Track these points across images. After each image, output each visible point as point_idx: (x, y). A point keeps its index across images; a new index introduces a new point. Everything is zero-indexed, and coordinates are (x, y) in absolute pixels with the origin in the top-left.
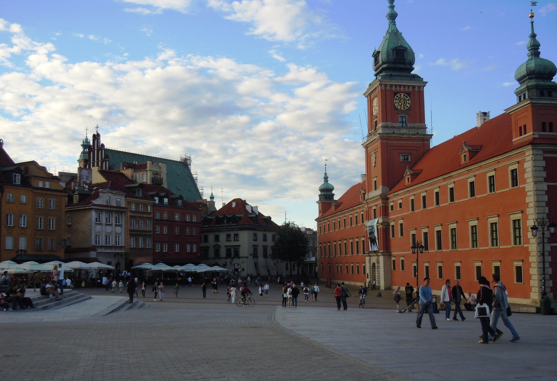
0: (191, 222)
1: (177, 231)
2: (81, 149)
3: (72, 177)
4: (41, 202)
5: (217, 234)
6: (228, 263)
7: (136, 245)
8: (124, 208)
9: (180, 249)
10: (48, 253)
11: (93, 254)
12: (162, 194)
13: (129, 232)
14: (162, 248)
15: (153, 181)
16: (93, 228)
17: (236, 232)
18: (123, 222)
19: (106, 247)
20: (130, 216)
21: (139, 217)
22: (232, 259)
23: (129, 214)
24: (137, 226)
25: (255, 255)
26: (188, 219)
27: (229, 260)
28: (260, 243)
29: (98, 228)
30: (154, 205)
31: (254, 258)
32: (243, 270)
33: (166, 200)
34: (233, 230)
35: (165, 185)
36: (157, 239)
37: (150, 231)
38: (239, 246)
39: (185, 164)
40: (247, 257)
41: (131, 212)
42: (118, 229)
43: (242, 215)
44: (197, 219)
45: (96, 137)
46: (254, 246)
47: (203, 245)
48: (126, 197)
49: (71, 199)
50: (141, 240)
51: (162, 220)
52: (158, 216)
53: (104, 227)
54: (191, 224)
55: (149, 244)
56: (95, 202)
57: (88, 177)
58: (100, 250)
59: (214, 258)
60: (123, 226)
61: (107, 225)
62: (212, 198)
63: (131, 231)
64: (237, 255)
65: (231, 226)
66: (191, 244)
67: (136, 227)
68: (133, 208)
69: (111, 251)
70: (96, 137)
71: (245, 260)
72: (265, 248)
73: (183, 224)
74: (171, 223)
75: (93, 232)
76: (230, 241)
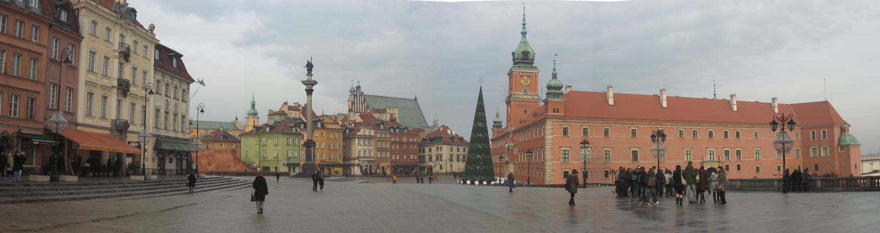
1: (405, 147)
3: (346, 118)
11: (357, 162)
25: (451, 160)
28: (455, 152)
29: (360, 148)
33: (397, 130)
35: (398, 121)
36: (393, 152)
45: (358, 88)
47: (422, 154)
49: (345, 132)
50: (384, 153)
52: (393, 139)
54: (413, 143)
68: (379, 135)
70: (358, 88)
72: (458, 156)
73: (408, 143)
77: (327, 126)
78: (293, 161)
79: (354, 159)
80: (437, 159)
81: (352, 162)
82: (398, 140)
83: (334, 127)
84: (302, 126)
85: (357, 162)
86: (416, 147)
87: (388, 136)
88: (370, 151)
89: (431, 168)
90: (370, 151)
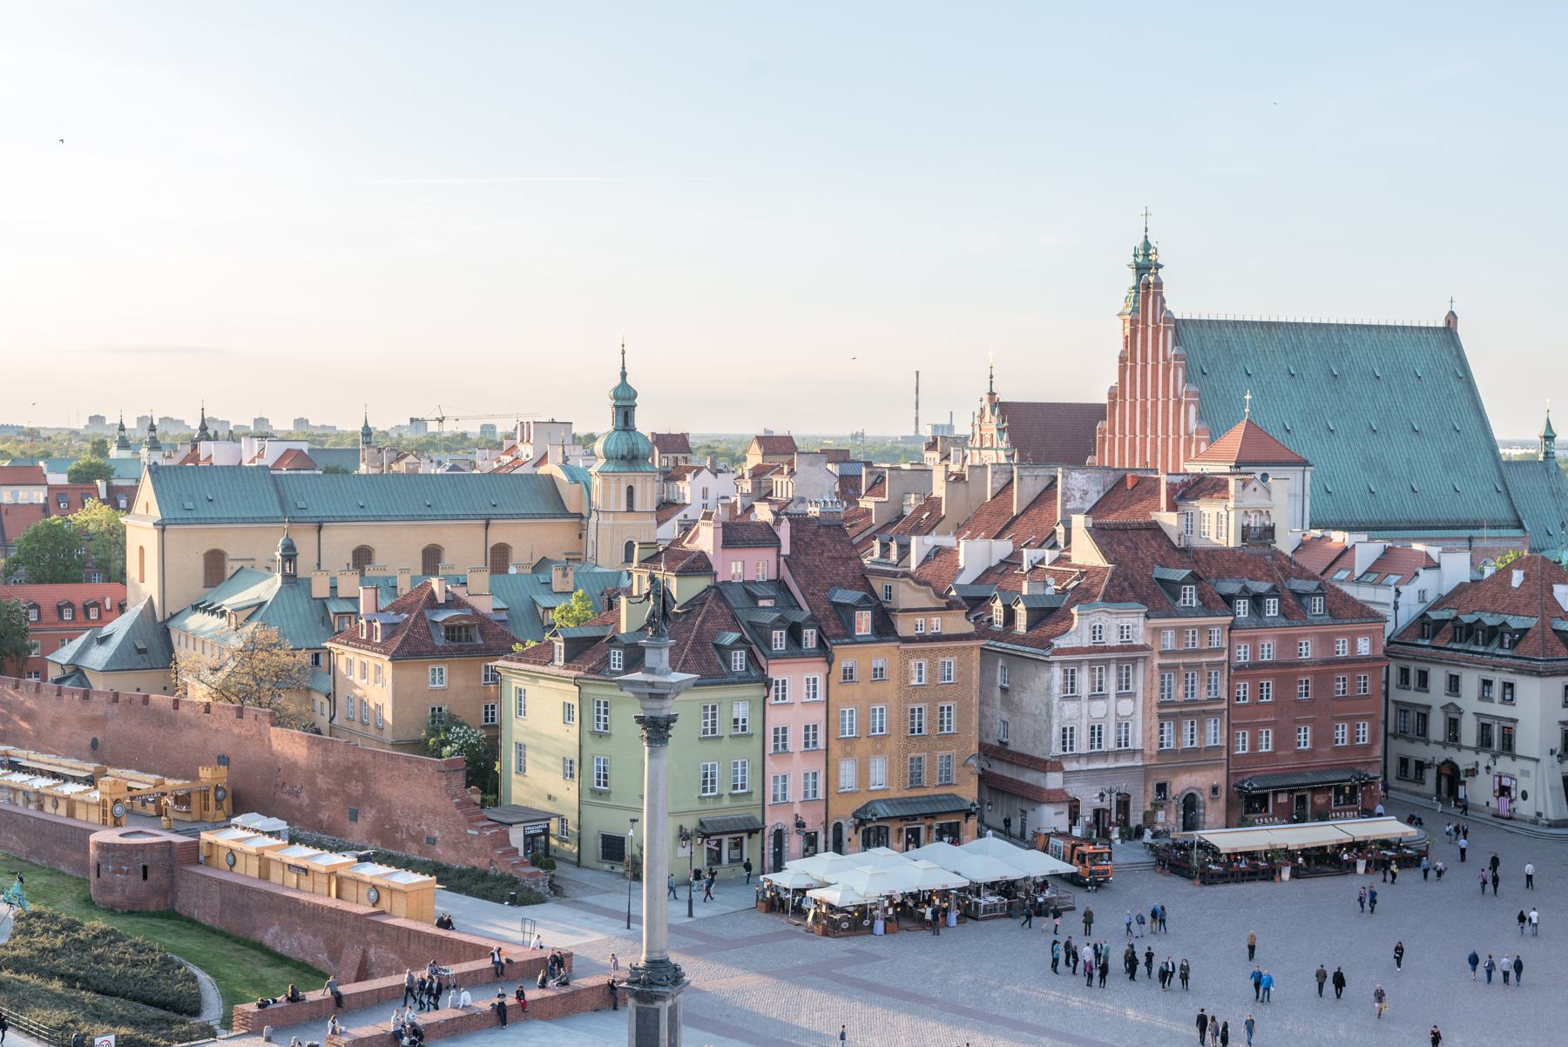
0: (1355, 661)
1: (1303, 688)
2: (1131, 279)
4: (918, 671)
5: (1454, 671)
6: (1482, 769)
7: (1177, 744)
8: (1143, 648)
9: (1314, 742)
10: (937, 792)
11: (1053, 781)
12: (1262, 587)
13: (1155, 710)
14: (1254, 745)
15: (1243, 540)
16: (1054, 713)
17: (1510, 678)
18: (1140, 684)
19: (1090, 757)
20: (1161, 667)
21: (1185, 665)
22: (1495, 757)
23: (1157, 661)
24: (1181, 692)
26: (1342, 649)
27: (1484, 759)
29: (1070, 708)
30: (1232, 627)
31: (1561, 758)
32: (1525, 796)
34: (1496, 668)
37: (1220, 700)
38: (1515, 721)
39: (1449, 332)
40: (1537, 760)
41: (1163, 654)
42: (1126, 706)
43: (1531, 623)
44: (1373, 646)
46: (1562, 723)
47: (1412, 696)
48: (1147, 617)
51: (1255, 666)
52: (1243, 654)
53: (1085, 706)
55: (1214, 733)
56: (1060, 643)
57: (1085, 493)
58: (1074, 766)
59: (1444, 745)
60: (1140, 695)
61: (1092, 697)
62: (1549, 437)
63: (1161, 705)
64: (1508, 746)
65: (1493, 655)
66: (1353, 720)
67: (1179, 694)
69: (1103, 765)
71: (1531, 766)
74: (1285, 669)
75: (1055, 721)
76: (1492, 701)
77: (904, 626)
78: (726, 809)
79: (1041, 765)
80: (1485, 729)
81: (1030, 777)
82: (1269, 651)
83: (937, 624)
84: (779, 638)
85: (1053, 781)
86: (1367, 683)
87: (1219, 639)
88: (1123, 725)
89: (1451, 778)
90: (1123, 725)
